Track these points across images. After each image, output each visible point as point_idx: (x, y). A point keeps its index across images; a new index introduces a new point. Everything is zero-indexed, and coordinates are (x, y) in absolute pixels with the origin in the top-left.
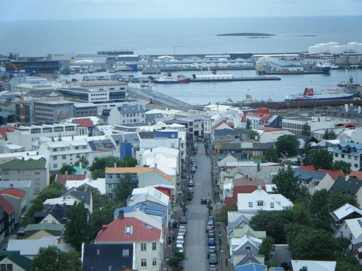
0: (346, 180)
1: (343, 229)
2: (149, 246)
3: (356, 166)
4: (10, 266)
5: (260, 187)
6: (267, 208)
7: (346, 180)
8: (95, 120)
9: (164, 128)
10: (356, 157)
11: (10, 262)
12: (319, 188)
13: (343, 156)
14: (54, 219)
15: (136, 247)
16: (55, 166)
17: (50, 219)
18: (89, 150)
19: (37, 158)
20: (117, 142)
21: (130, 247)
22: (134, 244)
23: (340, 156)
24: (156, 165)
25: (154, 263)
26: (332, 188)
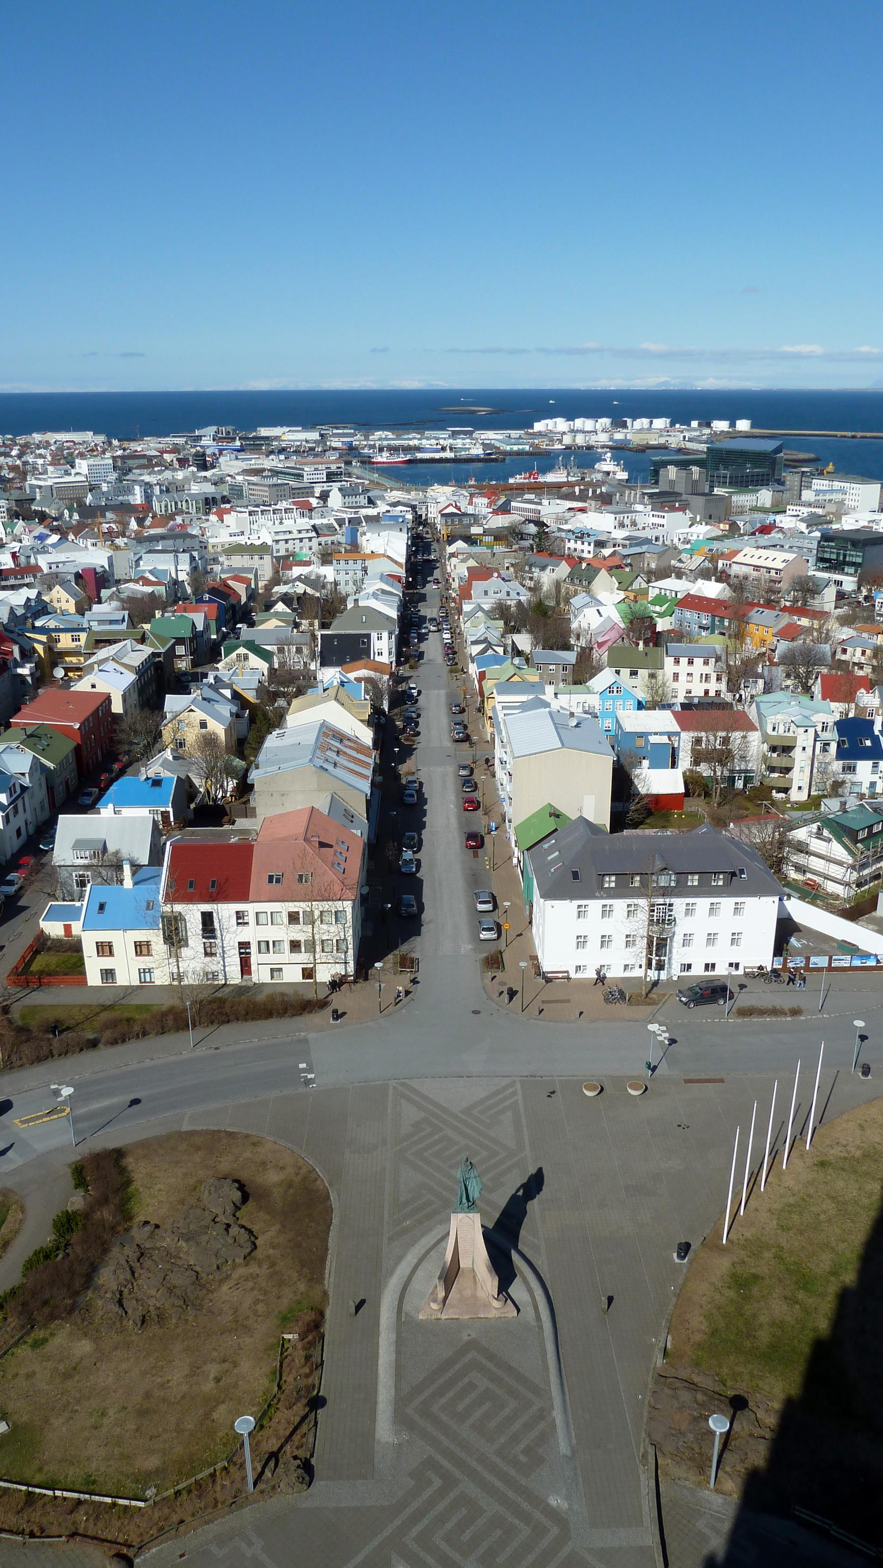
0: (583, 568)
1: (580, 618)
2: (385, 635)
3: (589, 552)
4: (246, 658)
5: (496, 575)
6: (502, 595)
7: (583, 568)
8: (314, 502)
9: (388, 511)
10: (589, 544)
11: (246, 652)
12: (554, 576)
13: (576, 541)
14: (285, 607)
15: (374, 635)
16: (278, 551)
17: (280, 607)
18: (314, 534)
19: (258, 543)
20: (340, 526)
21: (368, 636)
22: (372, 634)
23: (572, 541)
24: (385, 550)
25: (390, 653)
26: (568, 577)
